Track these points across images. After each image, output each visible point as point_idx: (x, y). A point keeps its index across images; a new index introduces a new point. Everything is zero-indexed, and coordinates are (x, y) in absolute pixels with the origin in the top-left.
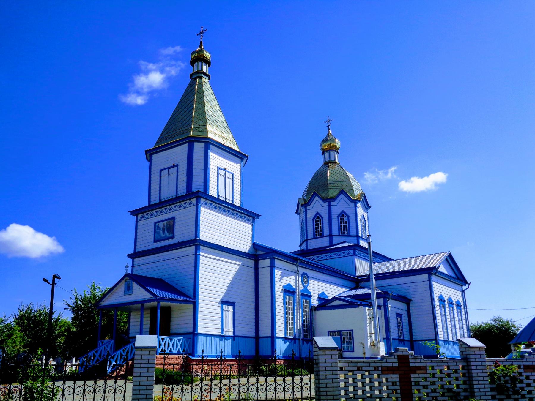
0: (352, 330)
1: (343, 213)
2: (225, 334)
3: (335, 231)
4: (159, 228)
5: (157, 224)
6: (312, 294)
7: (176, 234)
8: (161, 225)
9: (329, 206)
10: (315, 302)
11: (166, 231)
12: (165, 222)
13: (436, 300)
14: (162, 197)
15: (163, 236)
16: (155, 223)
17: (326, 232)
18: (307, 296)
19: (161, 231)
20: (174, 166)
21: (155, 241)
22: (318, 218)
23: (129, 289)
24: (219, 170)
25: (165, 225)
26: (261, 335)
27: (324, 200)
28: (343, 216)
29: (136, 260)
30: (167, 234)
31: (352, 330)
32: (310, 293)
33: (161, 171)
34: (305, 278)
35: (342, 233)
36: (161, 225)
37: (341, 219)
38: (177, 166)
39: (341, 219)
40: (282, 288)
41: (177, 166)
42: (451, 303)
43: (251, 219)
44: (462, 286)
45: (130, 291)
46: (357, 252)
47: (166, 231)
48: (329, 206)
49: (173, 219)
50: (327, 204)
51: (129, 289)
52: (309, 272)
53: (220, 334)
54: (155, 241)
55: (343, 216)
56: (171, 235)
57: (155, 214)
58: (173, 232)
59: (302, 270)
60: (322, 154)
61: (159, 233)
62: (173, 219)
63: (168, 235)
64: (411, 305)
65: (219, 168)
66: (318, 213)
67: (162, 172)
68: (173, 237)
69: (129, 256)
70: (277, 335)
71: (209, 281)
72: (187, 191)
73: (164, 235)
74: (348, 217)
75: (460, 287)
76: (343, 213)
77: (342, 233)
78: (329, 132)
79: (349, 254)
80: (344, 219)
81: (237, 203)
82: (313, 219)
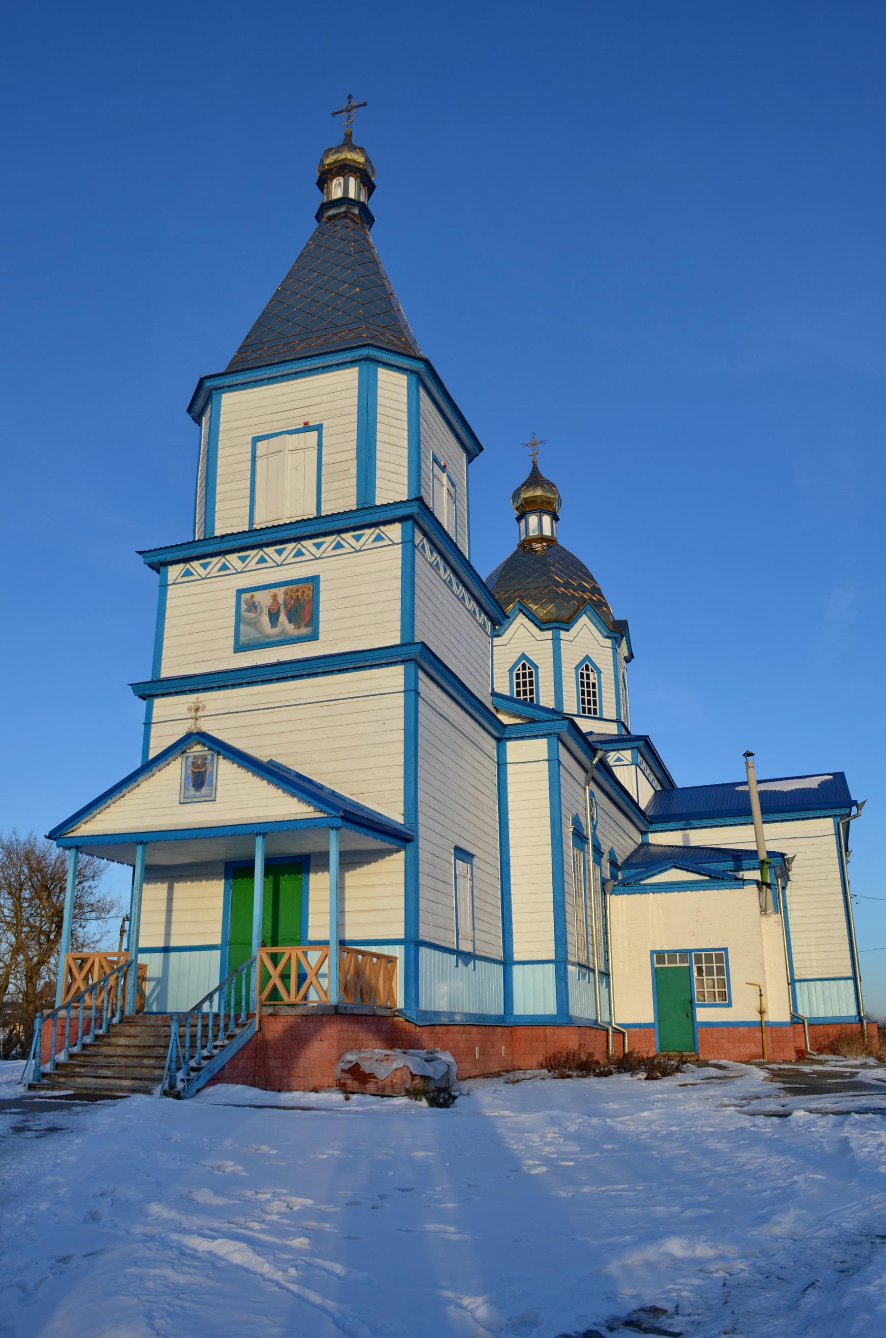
4: (253, 607)
5: (246, 596)
7: (322, 627)
9: (556, 640)
11: (283, 618)
12: (280, 592)
16: (240, 592)
19: (265, 619)
21: (239, 648)
25: (281, 599)
26: (516, 957)
27: (541, 624)
28: (587, 669)
29: (158, 702)
30: (290, 628)
31: (725, 949)
33: (256, 440)
35: (584, 708)
36: (264, 599)
37: (582, 674)
38: (319, 428)
39: (582, 674)
41: (319, 428)
45: (204, 790)
47: (283, 618)
48: (556, 640)
49: (314, 581)
50: (549, 634)
51: (199, 779)
54: (239, 648)
55: (587, 666)
56: (304, 631)
57: (239, 565)
58: (313, 621)
60: (518, 519)
61: (253, 624)
62: (314, 581)
67: (261, 446)
68: (314, 636)
73: (276, 631)
74: (599, 672)
77: (584, 708)
78: (535, 467)
79: (619, 759)
80: (588, 676)
82: (511, 671)
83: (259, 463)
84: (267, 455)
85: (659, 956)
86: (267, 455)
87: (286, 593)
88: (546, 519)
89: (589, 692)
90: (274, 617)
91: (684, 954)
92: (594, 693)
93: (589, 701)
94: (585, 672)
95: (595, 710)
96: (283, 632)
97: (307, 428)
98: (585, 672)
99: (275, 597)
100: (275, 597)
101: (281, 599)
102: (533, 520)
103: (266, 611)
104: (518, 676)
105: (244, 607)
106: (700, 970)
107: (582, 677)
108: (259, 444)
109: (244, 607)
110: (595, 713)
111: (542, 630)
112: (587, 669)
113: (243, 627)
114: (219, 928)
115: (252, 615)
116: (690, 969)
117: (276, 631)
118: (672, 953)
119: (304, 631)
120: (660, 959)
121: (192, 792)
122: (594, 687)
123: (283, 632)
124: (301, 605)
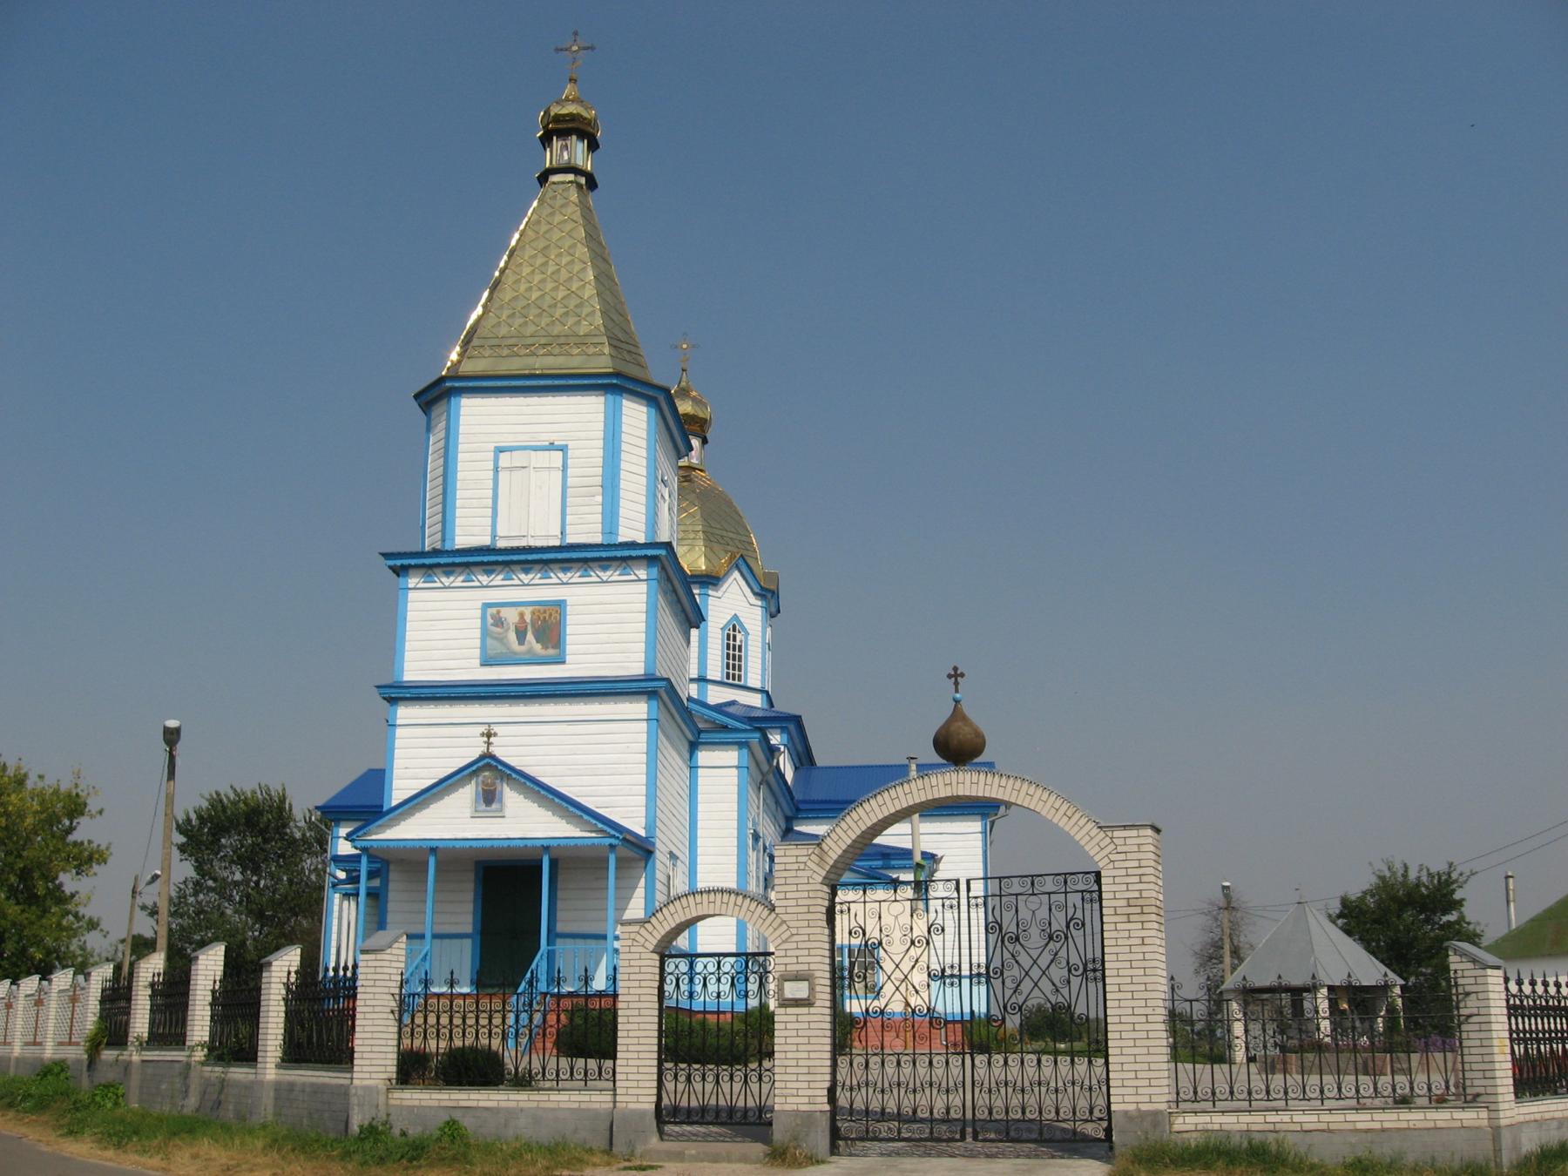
3: (715, 671)
4: (499, 622)
5: (494, 610)
8: (511, 616)
11: (530, 637)
14: (500, 532)
16: (486, 606)
19: (512, 636)
20: (551, 447)
23: (489, 797)
25: (528, 618)
30: (538, 647)
33: (500, 450)
36: (511, 616)
38: (563, 449)
45: (494, 806)
47: (530, 637)
49: (560, 605)
51: (489, 797)
54: (486, 662)
61: (501, 639)
62: (560, 605)
67: (505, 460)
68: (561, 661)
83: (501, 475)
84: (511, 469)
86: (511, 469)
87: (533, 613)
90: (521, 635)
96: (530, 651)
97: (551, 447)
99: (522, 615)
100: (522, 615)
101: (528, 618)
103: (512, 628)
108: (502, 455)
109: (490, 621)
114: (470, 918)
119: (551, 652)
121: (483, 807)
123: (530, 651)
124: (548, 628)
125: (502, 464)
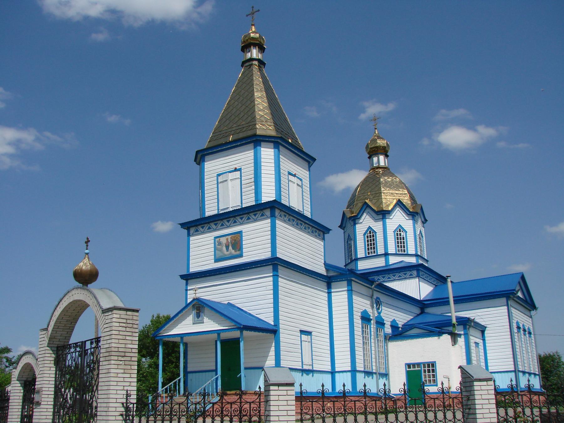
0: (435, 362)
1: (400, 229)
2: (305, 367)
3: (392, 249)
4: (220, 244)
5: (218, 239)
6: (385, 322)
10: (388, 330)
11: (230, 248)
12: (229, 237)
13: (515, 325)
14: (221, 208)
15: (226, 253)
16: (216, 238)
17: (381, 251)
18: (380, 323)
19: (224, 248)
20: (236, 170)
22: (370, 232)
24: (290, 176)
25: (229, 240)
26: (337, 370)
28: (400, 230)
30: (233, 251)
31: (435, 362)
32: (383, 320)
33: (219, 175)
34: (378, 303)
36: (223, 240)
37: (397, 234)
38: (240, 170)
39: (397, 234)
40: (360, 314)
41: (240, 170)
42: (524, 330)
43: (322, 234)
44: (530, 311)
46: (421, 273)
47: (230, 248)
49: (240, 233)
52: (383, 298)
53: (301, 368)
54: (217, 260)
55: (400, 230)
56: (238, 253)
57: (214, 227)
59: (376, 295)
60: (369, 158)
61: (221, 250)
62: (240, 233)
63: (232, 251)
64: (486, 332)
65: (290, 174)
66: (370, 228)
68: (241, 256)
69: (182, 277)
70: (358, 369)
71: (297, 306)
72: (256, 200)
73: (228, 253)
75: (528, 313)
76: (400, 229)
80: (400, 234)
81: (308, 214)
82: (364, 234)
85: (409, 365)
88: (382, 158)
89: (401, 242)
90: (227, 247)
91: (419, 364)
92: (404, 242)
93: (401, 246)
94: (399, 233)
95: (404, 250)
96: (231, 253)
97: (236, 170)
98: (399, 233)
99: (227, 239)
100: (227, 239)
102: (375, 159)
103: (224, 245)
104: (367, 236)
105: (217, 244)
106: (425, 371)
107: (397, 235)
108: (219, 178)
109: (217, 244)
110: (404, 252)
111: (378, 215)
112: (400, 231)
113: (217, 252)
115: (220, 247)
116: (420, 371)
117: (228, 253)
118: (414, 365)
119: (238, 253)
120: (409, 367)
121: (196, 319)
122: (403, 239)
123: (231, 253)
124: (236, 243)
125: (219, 181)
